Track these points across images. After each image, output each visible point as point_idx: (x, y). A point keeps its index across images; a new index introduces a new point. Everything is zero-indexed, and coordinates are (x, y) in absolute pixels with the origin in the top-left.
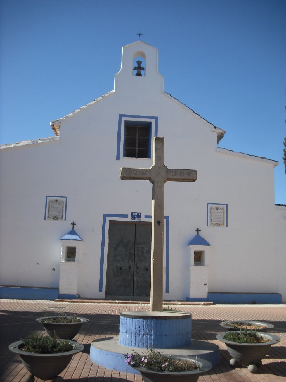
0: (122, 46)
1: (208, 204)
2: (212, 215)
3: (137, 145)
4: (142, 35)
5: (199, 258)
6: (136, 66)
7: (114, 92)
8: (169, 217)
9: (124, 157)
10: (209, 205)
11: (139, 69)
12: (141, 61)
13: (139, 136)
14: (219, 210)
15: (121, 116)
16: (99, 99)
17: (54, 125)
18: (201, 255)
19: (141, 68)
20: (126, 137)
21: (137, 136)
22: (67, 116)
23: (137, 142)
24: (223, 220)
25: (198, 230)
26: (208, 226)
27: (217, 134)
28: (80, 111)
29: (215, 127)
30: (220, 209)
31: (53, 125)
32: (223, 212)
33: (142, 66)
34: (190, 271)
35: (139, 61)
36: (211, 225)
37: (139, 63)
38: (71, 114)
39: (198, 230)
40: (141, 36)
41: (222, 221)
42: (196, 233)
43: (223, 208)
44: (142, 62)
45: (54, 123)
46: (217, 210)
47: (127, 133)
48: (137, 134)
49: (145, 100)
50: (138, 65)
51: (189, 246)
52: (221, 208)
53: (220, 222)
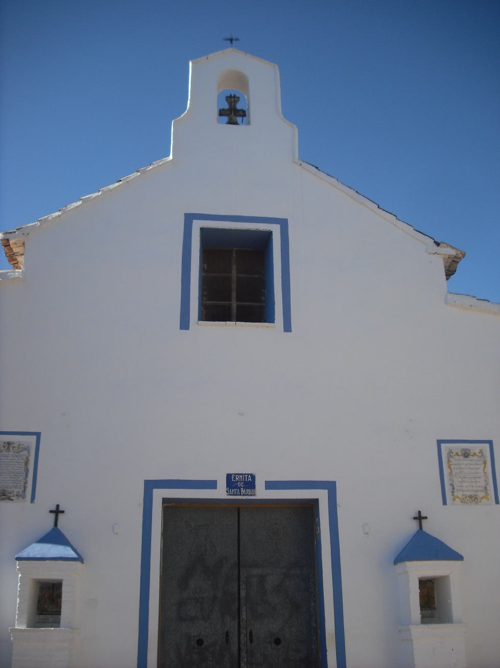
0: (191, 59)
1: (440, 442)
2: (453, 473)
3: (234, 294)
4: (237, 40)
5: (431, 599)
6: (226, 106)
7: (171, 160)
8: (334, 483)
9: (200, 322)
10: (443, 446)
11: (233, 112)
12: (237, 95)
13: (237, 273)
14: (470, 457)
15: (189, 219)
16: (133, 177)
17: (11, 242)
18: (432, 589)
19: (239, 111)
20: (203, 274)
21: (234, 272)
22: (46, 217)
23: (234, 286)
24: (483, 484)
25: (420, 518)
26: (445, 503)
27: (444, 259)
28: (80, 205)
29: (438, 244)
30: (475, 453)
31: (8, 240)
32: (482, 462)
33: (239, 106)
34: (411, 640)
35: (233, 95)
36: (454, 500)
37: (232, 99)
38: (58, 213)
39: (420, 518)
40: (234, 42)
41: (482, 489)
42: (413, 526)
43: (481, 452)
44: (239, 98)
45: (8, 236)
46: (466, 457)
47: (205, 265)
48: (234, 267)
49: (251, 172)
50: (230, 103)
51: (400, 566)
52: (477, 451)
53: (477, 491)
